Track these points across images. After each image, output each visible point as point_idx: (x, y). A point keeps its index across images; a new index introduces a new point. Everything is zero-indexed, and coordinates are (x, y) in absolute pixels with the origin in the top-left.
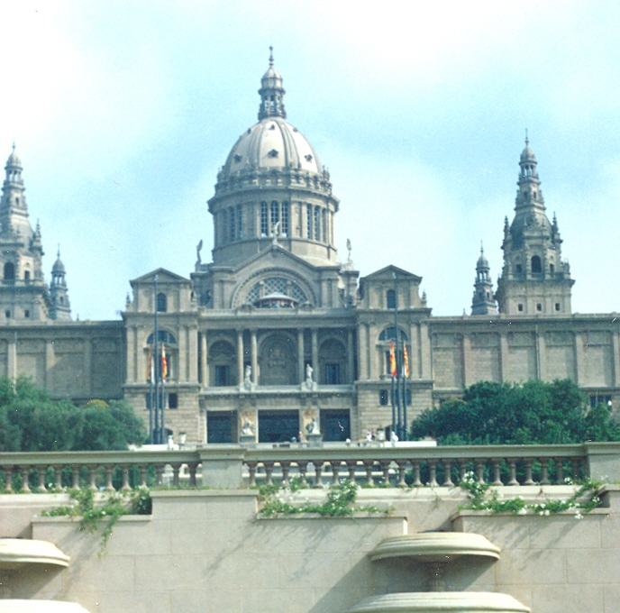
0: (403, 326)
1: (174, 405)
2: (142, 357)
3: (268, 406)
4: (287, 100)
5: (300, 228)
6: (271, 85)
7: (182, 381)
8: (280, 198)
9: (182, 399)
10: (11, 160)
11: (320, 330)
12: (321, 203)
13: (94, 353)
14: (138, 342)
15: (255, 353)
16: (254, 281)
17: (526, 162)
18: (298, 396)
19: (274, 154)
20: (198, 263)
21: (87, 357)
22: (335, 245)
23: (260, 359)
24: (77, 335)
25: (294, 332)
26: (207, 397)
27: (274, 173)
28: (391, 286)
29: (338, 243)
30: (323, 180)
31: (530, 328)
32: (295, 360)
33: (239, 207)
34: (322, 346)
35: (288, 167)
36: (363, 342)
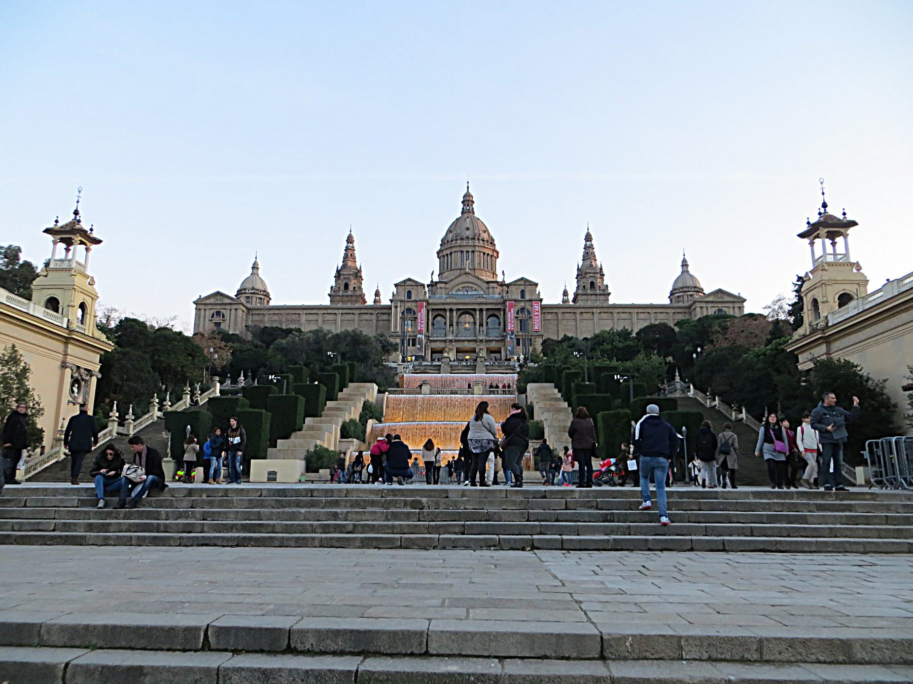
0: (529, 308)
1: (414, 345)
3: (459, 345)
5: (480, 264)
6: (467, 198)
8: (470, 249)
13: (378, 321)
15: (455, 320)
17: (588, 238)
18: (475, 341)
19: (468, 229)
21: (375, 321)
22: (497, 273)
23: (457, 323)
24: (370, 311)
25: (474, 310)
26: (431, 341)
27: (468, 238)
28: (522, 287)
31: (591, 310)
32: (475, 323)
35: (475, 235)
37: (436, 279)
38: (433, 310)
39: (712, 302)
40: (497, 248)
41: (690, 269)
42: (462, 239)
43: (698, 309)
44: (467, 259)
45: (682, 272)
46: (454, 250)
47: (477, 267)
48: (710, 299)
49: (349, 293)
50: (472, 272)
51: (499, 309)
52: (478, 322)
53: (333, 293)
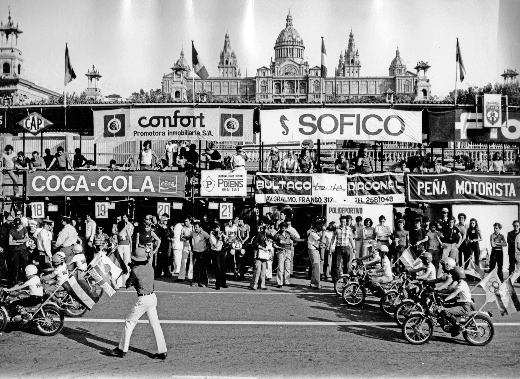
2: (260, 86)
4: (293, 22)
6: (289, 18)
7: (269, 92)
9: (269, 96)
10: (226, 35)
11: (300, 81)
12: (301, 48)
20: (272, 62)
25: (294, 81)
27: (290, 41)
29: (304, 57)
30: (301, 42)
32: (294, 87)
33: (281, 49)
36: (310, 84)
37: (273, 61)
39: (404, 77)
40: (304, 45)
42: (287, 42)
43: (397, 81)
44: (290, 52)
45: (396, 57)
47: (294, 56)
48: (403, 75)
49: (229, 65)
50: (292, 59)
52: (296, 87)
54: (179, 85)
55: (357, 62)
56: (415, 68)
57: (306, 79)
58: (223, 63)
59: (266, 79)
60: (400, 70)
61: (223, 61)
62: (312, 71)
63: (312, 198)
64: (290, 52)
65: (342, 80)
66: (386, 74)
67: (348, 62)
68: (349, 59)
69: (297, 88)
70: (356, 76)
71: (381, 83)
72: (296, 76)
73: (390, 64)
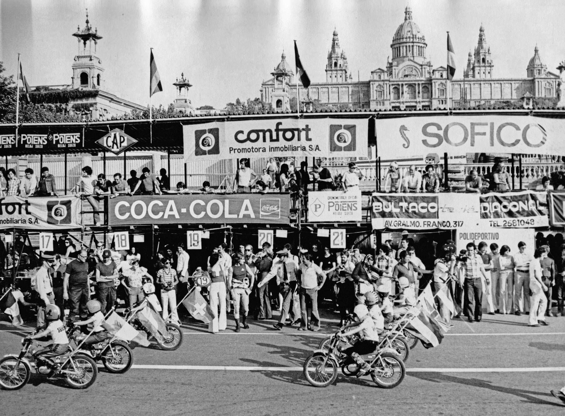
2: (375, 92)
4: (413, 15)
6: (408, 10)
7: (385, 98)
9: (385, 102)
10: (334, 32)
12: (423, 45)
14: (374, 88)
16: (404, 68)
25: (415, 84)
27: (409, 37)
32: (415, 92)
33: (400, 47)
34: (423, 87)
35: (413, 35)
37: (390, 61)
38: (393, 85)
40: (426, 42)
41: (539, 52)
42: (406, 38)
43: (537, 83)
44: (410, 51)
45: (535, 55)
46: (401, 45)
47: (415, 54)
48: (543, 77)
49: (338, 68)
50: (412, 58)
51: (428, 84)
53: (328, 69)
54: (280, 92)
55: (490, 62)
56: (557, 68)
57: (430, 82)
58: (331, 65)
59: (381, 83)
60: (539, 70)
61: (331, 63)
62: (436, 72)
63: (438, 222)
64: (410, 51)
65: (472, 83)
66: (524, 75)
67: (479, 61)
68: (480, 58)
69: (419, 93)
70: (488, 77)
71: (517, 85)
72: (418, 79)
73: (527, 64)
